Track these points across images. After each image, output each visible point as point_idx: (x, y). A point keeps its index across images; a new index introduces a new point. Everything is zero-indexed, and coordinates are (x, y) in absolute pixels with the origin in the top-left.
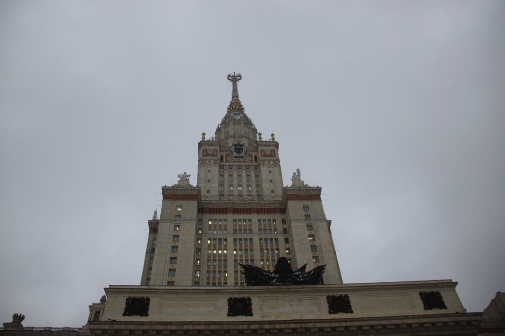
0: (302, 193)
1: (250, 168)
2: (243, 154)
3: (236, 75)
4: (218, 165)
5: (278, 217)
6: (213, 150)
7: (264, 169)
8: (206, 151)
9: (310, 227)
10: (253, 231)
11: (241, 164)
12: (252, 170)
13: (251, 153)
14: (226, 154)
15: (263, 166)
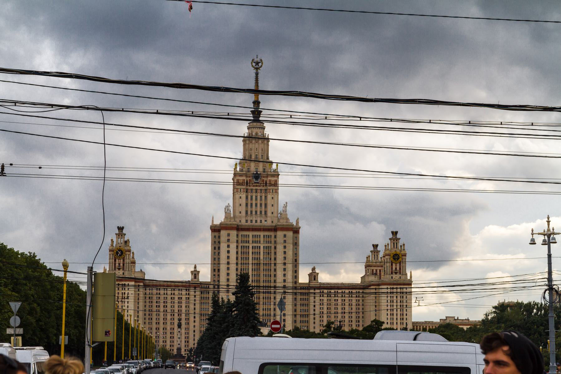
0: (285, 227)
1: (262, 192)
2: (259, 180)
3: (258, 60)
4: (245, 193)
5: (272, 234)
6: (242, 181)
7: (269, 197)
8: (239, 181)
9: (285, 247)
10: (261, 243)
11: (257, 188)
12: (263, 193)
13: (263, 179)
14: (249, 180)
15: (269, 194)
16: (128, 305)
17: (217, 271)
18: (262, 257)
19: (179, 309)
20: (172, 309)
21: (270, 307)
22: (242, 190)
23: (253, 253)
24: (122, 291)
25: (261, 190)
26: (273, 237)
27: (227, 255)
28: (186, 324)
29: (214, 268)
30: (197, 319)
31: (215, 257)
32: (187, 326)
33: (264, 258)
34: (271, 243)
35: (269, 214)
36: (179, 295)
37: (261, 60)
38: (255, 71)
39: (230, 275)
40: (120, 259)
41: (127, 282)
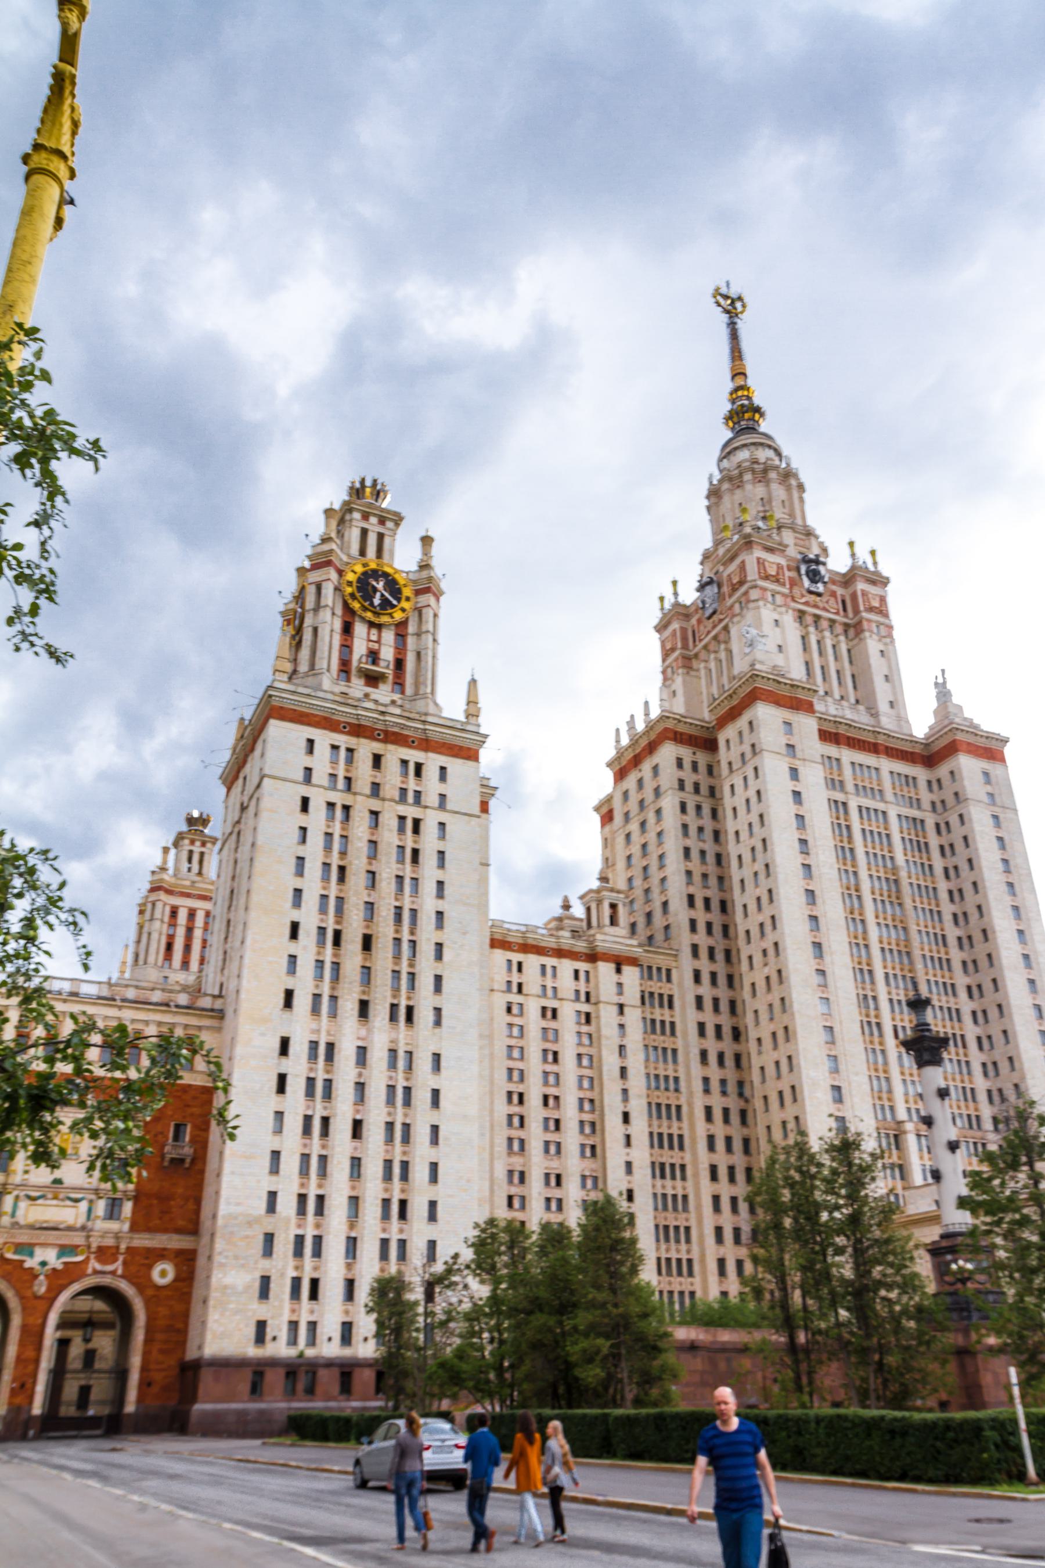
5: (919, 773)
7: (872, 645)
13: (834, 588)
16: (441, 905)
17: (699, 903)
18: (900, 859)
19: (550, 1068)
20: (512, 1064)
21: (971, 1082)
22: (778, 598)
23: (863, 830)
24: (402, 810)
25: (832, 622)
26: (922, 784)
27: (793, 809)
28: (583, 1154)
29: (692, 890)
30: (640, 1127)
31: (689, 843)
32: (589, 1166)
33: (907, 861)
34: (919, 808)
35: (883, 707)
36: (544, 995)
37: (740, 299)
38: (725, 318)
39: (819, 901)
40: (379, 627)
41: (431, 755)
